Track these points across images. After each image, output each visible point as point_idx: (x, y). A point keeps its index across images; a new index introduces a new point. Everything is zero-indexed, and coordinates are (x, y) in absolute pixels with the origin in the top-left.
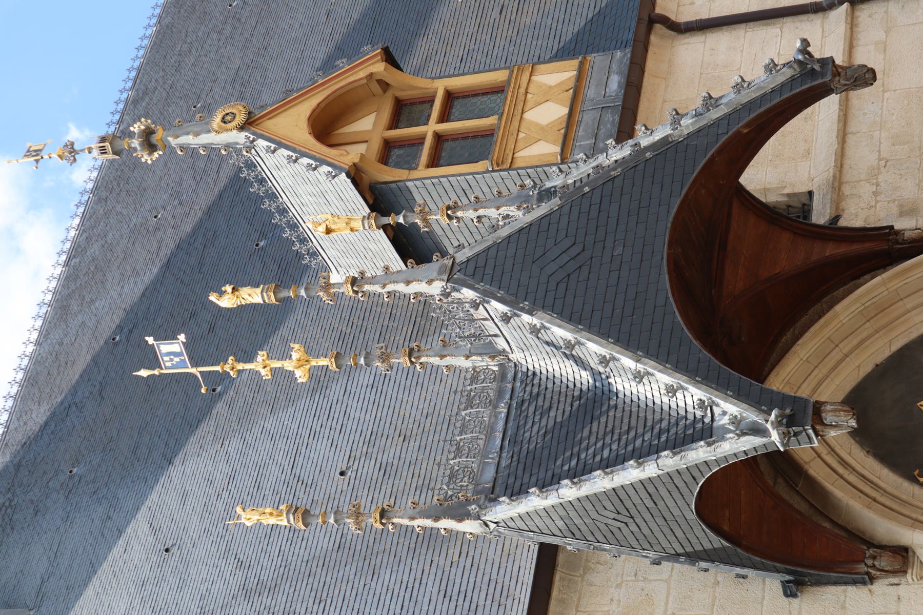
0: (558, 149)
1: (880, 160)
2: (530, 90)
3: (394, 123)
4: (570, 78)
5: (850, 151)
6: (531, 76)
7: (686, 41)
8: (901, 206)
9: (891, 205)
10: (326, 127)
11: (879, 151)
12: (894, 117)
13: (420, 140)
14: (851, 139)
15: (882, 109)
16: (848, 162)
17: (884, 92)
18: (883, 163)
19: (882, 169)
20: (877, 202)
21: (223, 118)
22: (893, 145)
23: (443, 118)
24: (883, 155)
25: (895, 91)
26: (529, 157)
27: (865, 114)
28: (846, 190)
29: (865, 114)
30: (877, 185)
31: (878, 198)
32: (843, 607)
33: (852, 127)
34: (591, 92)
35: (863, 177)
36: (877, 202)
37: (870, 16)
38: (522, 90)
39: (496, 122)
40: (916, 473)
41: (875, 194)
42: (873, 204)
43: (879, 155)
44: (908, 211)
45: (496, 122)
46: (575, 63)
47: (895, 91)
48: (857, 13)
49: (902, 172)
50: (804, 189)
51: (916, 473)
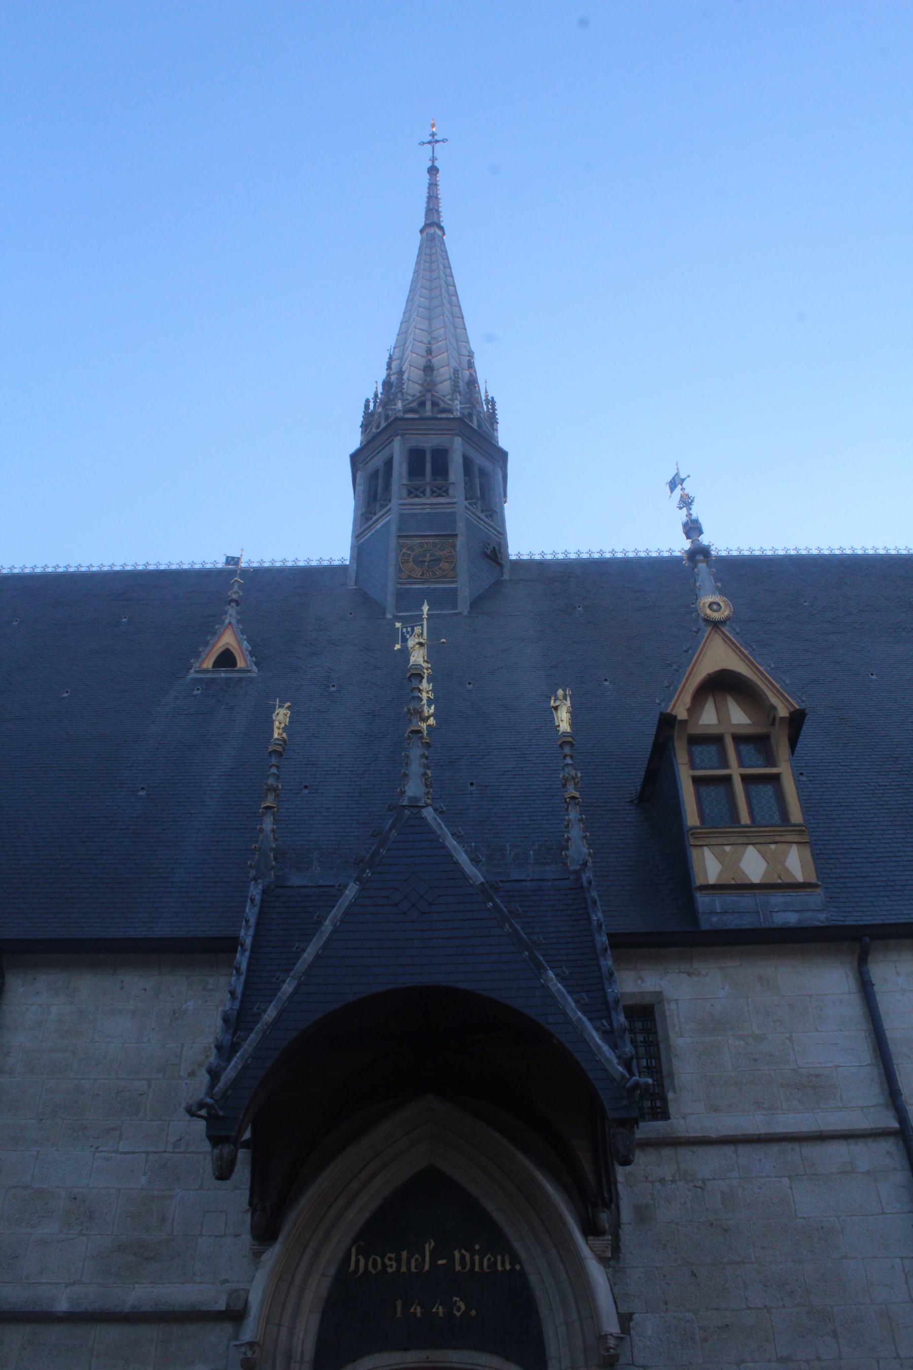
0: (712, 881)
1: (704, 1181)
2: (780, 846)
3: (739, 739)
4: (793, 876)
5: (713, 1151)
6: (796, 843)
7: (851, 976)
9: (649, 1197)
10: (722, 684)
11: (714, 1179)
13: (726, 765)
14: (728, 1150)
15: (767, 1176)
16: (700, 1150)
17: (789, 1177)
18: (700, 1184)
19: (692, 1184)
20: (652, 1183)
21: (714, 603)
22: (722, 1193)
23: (745, 778)
25: (791, 1188)
26: (704, 860)
27: (760, 1160)
28: (666, 1152)
29: (760, 1160)
30: (672, 1182)
31: (657, 1184)
32: (236, 1188)
33: (742, 1149)
34: (777, 899)
36: (652, 1183)
37: (888, 1153)
38: (778, 839)
39: (743, 822)
40: (362, 1243)
41: (662, 1181)
42: (650, 1178)
43: (708, 1180)
44: (643, 1215)
45: (743, 822)
46: (813, 879)
47: (791, 1188)
48: (891, 1140)
50: (672, 1110)
51: (362, 1243)
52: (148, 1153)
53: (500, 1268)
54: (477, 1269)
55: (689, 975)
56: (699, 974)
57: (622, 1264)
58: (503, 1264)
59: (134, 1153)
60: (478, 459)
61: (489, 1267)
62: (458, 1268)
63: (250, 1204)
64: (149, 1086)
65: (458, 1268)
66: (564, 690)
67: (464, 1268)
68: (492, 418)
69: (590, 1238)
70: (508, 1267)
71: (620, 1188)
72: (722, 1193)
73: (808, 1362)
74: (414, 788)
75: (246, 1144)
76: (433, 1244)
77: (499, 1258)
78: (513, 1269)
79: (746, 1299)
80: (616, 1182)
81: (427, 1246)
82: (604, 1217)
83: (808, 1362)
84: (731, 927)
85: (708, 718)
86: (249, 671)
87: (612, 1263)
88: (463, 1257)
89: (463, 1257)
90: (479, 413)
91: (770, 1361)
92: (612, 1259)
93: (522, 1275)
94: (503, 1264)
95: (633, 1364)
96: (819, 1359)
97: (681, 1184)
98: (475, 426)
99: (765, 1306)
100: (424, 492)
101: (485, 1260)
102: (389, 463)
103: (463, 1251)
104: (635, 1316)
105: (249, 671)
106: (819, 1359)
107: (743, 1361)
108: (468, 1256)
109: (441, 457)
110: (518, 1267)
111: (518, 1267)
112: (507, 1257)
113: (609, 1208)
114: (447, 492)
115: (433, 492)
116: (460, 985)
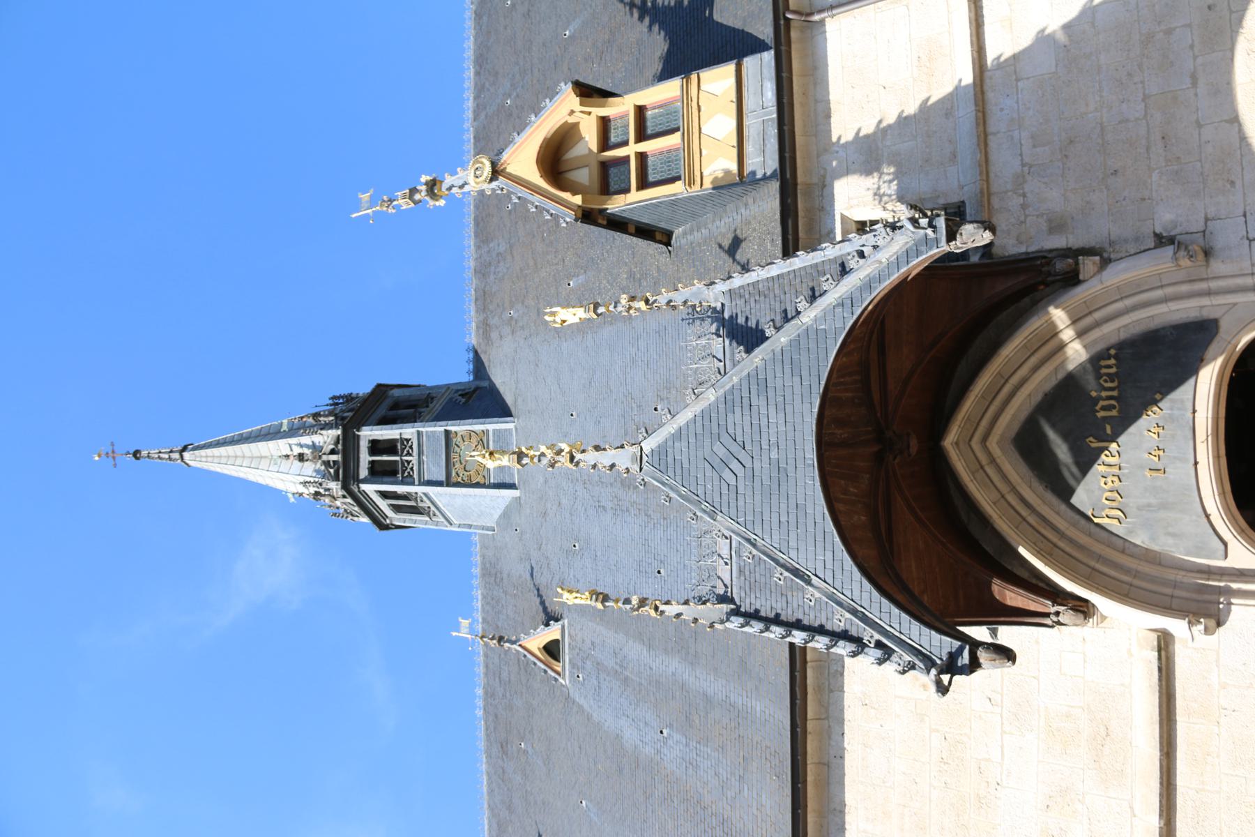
1: (1023, 165)
5: (993, 156)
8: (1050, 221)
11: (1021, 155)
12: (1031, 112)
13: (626, 160)
17: (1017, 80)
18: (1026, 169)
20: (1026, 216)
22: (1034, 146)
24: (1027, 160)
27: (1002, 110)
29: (1002, 110)
30: (1024, 195)
35: (1009, 187)
41: (1024, 206)
42: (1022, 218)
44: (1056, 226)
49: (1046, 180)
52: (1003, 732)
53: (1113, 370)
54: (1115, 393)
55: (824, 186)
56: (824, 177)
57: (1107, 245)
58: (1109, 367)
59: (1002, 747)
60: (382, 411)
61: (1112, 381)
62: (1114, 413)
63: (1052, 627)
64: (937, 731)
65: (1114, 413)
66: (546, 314)
67: (1114, 407)
68: (349, 398)
69: (1081, 277)
70: (1113, 361)
71: (1031, 249)
72: (1034, 146)
73: (1195, 58)
74: (624, 459)
75: (994, 633)
76: (1091, 439)
77: (1104, 371)
78: (1116, 357)
79: (1137, 119)
80: (1027, 253)
81: (1093, 445)
82: (1060, 265)
83: (1195, 58)
84: (776, 147)
85: (584, 176)
86: (563, 627)
87: (1105, 255)
88: (1104, 408)
89: (1104, 408)
90: (342, 411)
91: (1196, 95)
92: (1103, 256)
93: (1121, 346)
94: (1109, 367)
95: (1204, 232)
96: (1192, 47)
97: (1027, 188)
98: (350, 414)
99: (1143, 100)
100: (409, 462)
101: (1107, 385)
102: (385, 495)
103: (1098, 408)
104: (1158, 231)
105: (563, 627)
106: (1192, 47)
107: (1197, 122)
108: (1102, 403)
109: (376, 447)
110: (1113, 352)
111: (1113, 352)
112: (1103, 363)
113: (1051, 259)
114: (408, 440)
115: (409, 454)
116: (816, 410)
